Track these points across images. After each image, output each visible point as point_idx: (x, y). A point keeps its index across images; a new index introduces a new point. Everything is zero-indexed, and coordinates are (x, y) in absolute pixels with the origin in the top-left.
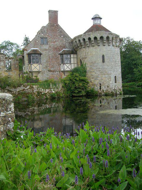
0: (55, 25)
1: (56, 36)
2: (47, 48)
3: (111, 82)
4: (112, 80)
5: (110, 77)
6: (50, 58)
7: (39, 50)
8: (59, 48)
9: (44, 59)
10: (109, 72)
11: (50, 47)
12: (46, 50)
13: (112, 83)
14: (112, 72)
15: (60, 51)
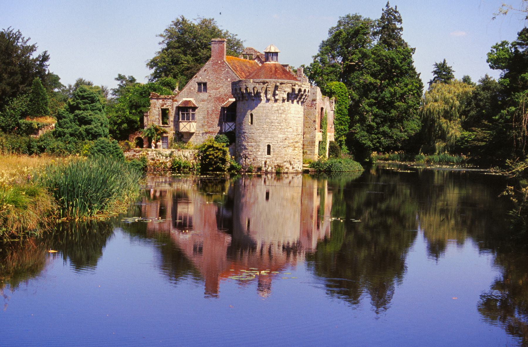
0: (220, 62)
1: (221, 79)
2: (206, 98)
3: (259, 153)
4: (261, 150)
5: (259, 146)
6: (208, 113)
7: (194, 102)
8: (223, 98)
9: (199, 114)
10: (258, 139)
11: (210, 96)
12: (203, 101)
13: (262, 155)
14: (263, 139)
15: (223, 101)
